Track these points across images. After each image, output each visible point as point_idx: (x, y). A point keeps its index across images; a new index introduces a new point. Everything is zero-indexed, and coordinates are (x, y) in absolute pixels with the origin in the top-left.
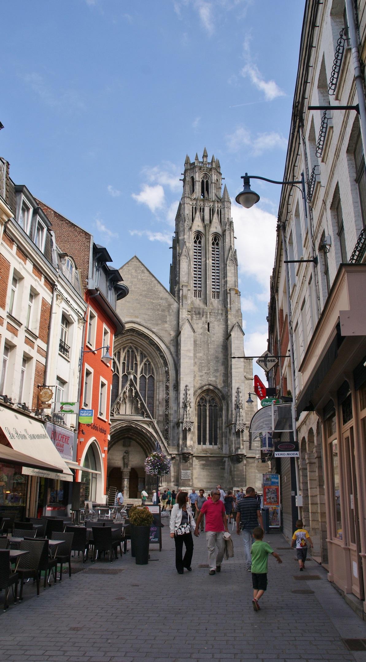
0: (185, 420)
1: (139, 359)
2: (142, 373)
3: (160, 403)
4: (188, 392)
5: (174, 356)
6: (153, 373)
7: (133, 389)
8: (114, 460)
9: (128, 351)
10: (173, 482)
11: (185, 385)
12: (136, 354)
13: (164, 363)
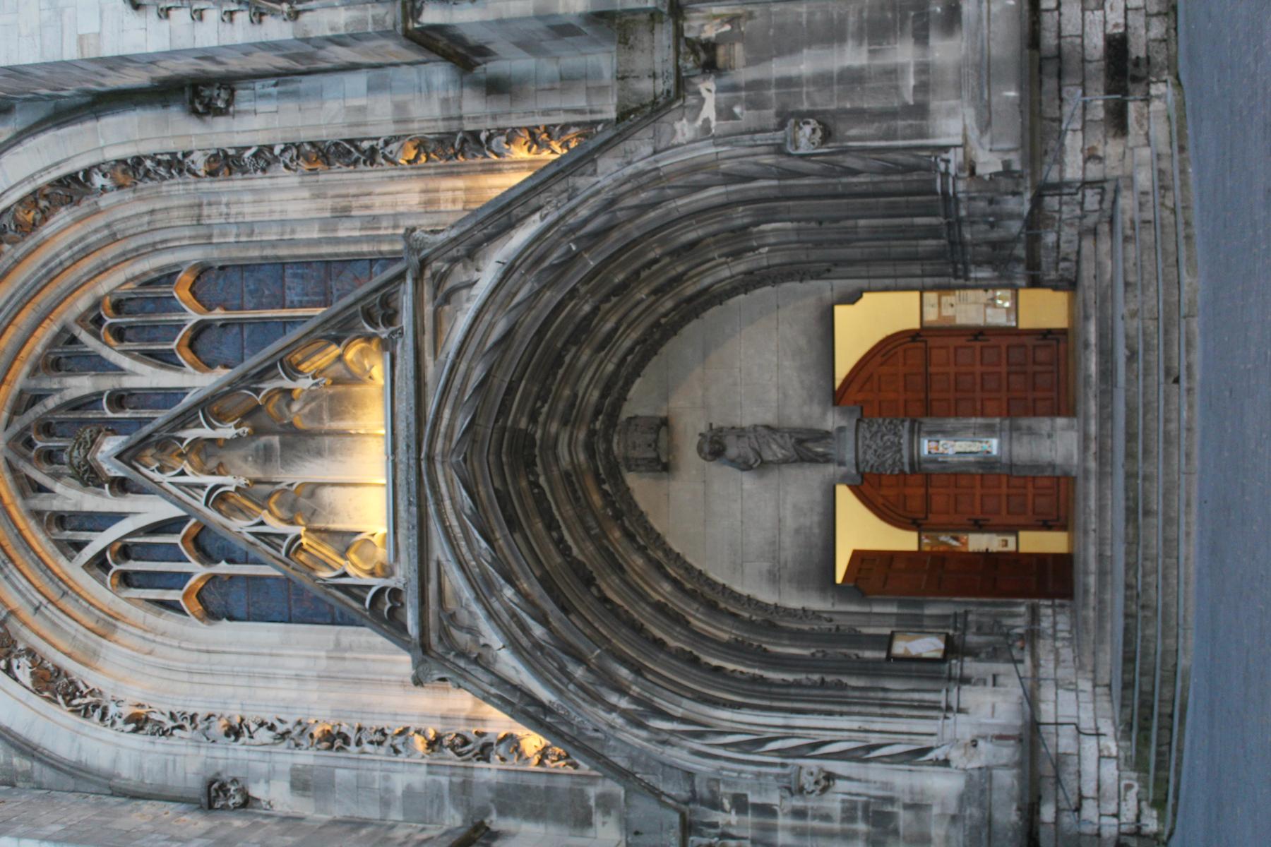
1: (81, 385)
2: (166, 360)
3: (343, 213)
6: (168, 276)
7: (190, 434)
9: (50, 456)
10: (921, 38)
12: (51, 402)
13: (71, 201)
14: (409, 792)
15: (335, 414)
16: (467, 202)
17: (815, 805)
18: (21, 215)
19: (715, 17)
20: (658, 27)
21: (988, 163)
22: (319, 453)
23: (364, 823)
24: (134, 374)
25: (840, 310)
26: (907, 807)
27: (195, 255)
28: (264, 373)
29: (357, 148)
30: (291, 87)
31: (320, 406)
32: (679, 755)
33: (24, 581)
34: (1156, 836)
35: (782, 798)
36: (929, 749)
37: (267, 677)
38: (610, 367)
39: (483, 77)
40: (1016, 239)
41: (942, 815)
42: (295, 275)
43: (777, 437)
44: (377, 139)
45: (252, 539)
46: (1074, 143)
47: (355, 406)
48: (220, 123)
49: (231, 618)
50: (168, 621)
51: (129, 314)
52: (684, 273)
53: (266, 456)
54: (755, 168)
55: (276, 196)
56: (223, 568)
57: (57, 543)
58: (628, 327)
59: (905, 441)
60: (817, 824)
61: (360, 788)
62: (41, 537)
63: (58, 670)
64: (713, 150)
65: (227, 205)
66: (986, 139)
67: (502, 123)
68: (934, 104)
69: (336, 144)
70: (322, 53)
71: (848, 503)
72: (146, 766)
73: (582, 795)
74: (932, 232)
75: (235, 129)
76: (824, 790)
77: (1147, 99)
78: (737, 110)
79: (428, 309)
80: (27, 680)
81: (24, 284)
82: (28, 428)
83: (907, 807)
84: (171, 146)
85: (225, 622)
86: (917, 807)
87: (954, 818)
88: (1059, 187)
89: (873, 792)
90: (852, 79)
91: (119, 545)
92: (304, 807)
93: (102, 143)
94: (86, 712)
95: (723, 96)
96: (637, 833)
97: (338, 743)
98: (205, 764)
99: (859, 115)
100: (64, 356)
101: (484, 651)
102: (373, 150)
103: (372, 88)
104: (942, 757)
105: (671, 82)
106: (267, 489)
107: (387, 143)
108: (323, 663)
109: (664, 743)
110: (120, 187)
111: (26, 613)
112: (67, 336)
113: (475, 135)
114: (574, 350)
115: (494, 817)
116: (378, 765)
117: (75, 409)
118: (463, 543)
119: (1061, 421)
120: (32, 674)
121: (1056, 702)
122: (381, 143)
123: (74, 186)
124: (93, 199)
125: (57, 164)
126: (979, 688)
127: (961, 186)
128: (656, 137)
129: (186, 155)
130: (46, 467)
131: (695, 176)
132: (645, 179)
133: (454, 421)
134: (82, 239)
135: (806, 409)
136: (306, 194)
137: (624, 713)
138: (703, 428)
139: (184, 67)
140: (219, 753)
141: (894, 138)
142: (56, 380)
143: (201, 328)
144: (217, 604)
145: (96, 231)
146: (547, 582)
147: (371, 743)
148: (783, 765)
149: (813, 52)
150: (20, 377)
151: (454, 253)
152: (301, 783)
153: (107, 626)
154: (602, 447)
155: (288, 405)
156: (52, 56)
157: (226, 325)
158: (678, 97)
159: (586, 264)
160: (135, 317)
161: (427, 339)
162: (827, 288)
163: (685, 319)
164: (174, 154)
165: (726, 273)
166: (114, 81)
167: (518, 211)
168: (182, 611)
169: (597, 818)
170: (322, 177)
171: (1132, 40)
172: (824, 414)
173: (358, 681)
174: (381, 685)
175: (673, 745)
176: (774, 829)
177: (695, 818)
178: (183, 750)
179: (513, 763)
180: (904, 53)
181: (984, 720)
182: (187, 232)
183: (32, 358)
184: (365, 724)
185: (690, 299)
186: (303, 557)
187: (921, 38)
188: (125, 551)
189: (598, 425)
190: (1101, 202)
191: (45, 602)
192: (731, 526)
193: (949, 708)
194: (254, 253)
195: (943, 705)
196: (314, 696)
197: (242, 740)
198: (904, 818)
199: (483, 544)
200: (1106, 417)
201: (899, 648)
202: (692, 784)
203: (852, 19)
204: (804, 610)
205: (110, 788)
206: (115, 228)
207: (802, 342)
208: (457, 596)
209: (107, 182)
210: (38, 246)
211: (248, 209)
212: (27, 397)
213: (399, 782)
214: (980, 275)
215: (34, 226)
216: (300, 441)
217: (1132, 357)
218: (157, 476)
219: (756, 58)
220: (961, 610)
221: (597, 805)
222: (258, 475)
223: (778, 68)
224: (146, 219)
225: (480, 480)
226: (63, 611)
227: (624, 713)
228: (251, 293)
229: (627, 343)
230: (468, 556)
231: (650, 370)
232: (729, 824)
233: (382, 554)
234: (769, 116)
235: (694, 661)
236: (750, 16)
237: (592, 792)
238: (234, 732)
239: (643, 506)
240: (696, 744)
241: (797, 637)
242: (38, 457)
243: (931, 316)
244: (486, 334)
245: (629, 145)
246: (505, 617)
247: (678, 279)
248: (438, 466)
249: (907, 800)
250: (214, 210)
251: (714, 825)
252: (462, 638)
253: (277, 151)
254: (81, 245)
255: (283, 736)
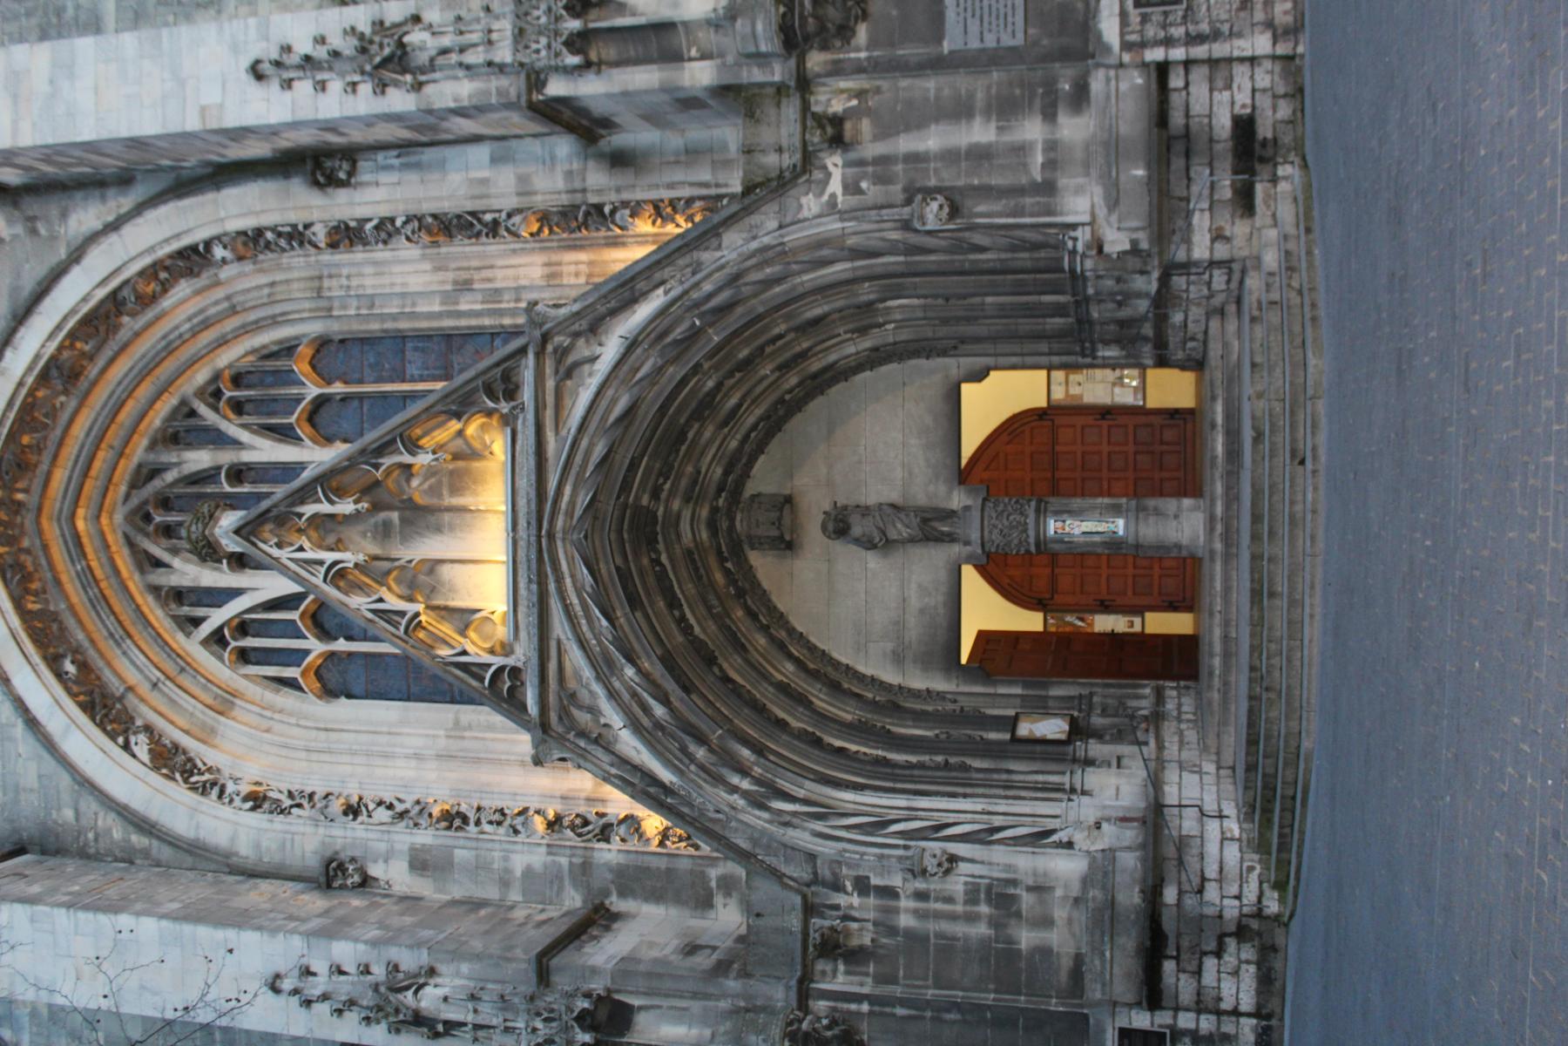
0: (504, 53)
1: (199, 459)
2: (284, 434)
3: (464, 286)
4: (304, 47)
5: (126, 202)
6: (288, 349)
7: (309, 510)
8: (899, 625)
9: (168, 531)
10: (1050, 116)
11: (253, 88)
12: (170, 476)
13: (191, 273)
14: (528, 872)
15: (455, 490)
16: (590, 276)
17: (939, 887)
18: (141, 287)
19: (842, 91)
20: (784, 101)
21: (1117, 241)
22: (439, 529)
23: (481, 904)
24: (252, 448)
25: (966, 388)
26: (1029, 889)
27: (315, 328)
28: (383, 448)
29: (479, 220)
30: (413, 159)
31: (440, 483)
32: (801, 837)
33: (142, 657)
34: (1277, 918)
35: (905, 880)
36: (1053, 832)
37: (386, 756)
38: (734, 444)
39: (607, 149)
40: (1144, 318)
41: (1065, 898)
42: (416, 349)
43: (902, 516)
44: (500, 211)
45: (370, 616)
46: (1201, 223)
47: (475, 482)
48: (342, 195)
49: (350, 696)
50: (286, 699)
51: (249, 387)
52: (810, 349)
53: (385, 532)
54: (880, 244)
55: (397, 269)
56: (341, 645)
57: (175, 618)
58: (753, 402)
59: (1031, 520)
60: (939, 906)
61: (480, 868)
62: (159, 612)
63: (176, 747)
64: (839, 225)
65: (348, 277)
66: (1114, 218)
67: (626, 196)
68: (1063, 182)
69: (459, 217)
70: (445, 125)
71: (973, 583)
72: (265, 844)
73: (703, 876)
74: (1059, 310)
75: (357, 200)
76: (947, 872)
77: (1274, 180)
78: (864, 185)
79: (550, 384)
80: (145, 757)
81: (143, 356)
82: (146, 502)
83: (1029, 889)
84: (294, 217)
85: (343, 700)
86: (1040, 889)
87: (1077, 900)
88: (1186, 267)
89: (996, 875)
90: (980, 155)
91: (237, 621)
92: (422, 887)
93: (223, 214)
94: (204, 789)
95: (850, 171)
96: (758, 915)
97: (457, 822)
98: (323, 843)
99: (986, 192)
100: (183, 430)
101: (604, 731)
102: (496, 222)
103: (495, 160)
104: (1065, 840)
105: (798, 156)
106: (386, 565)
107: (509, 216)
108: (442, 742)
109: (787, 824)
110: (240, 258)
111: (144, 689)
112: (185, 410)
113: (599, 208)
114: (696, 426)
115: (614, 898)
116: (497, 846)
117: (194, 483)
118: (583, 622)
119: (1187, 502)
120: (150, 751)
121: (1180, 784)
122: (504, 215)
123: (195, 258)
124: (212, 271)
125: (177, 236)
126: (1103, 770)
127: (1089, 264)
128: (781, 211)
129: (307, 226)
130: (164, 542)
131: (820, 251)
132: (770, 254)
133: (575, 498)
134: (202, 311)
135: (931, 488)
136: (427, 266)
137: (746, 794)
138: (827, 507)
139: (305, 138)
140: (337, 831)
141: (1022, 215)
142: (174, 454)
143: (321, 402)
144: (335, 681)
145: (216, 303)
146: (668, 661)
147: (490, 822)
148: (906, 847)
149: (940, 128)
150: (139, 451)
151: (576, 327)
152: (420, 863)
153: (225, 702)
154: (725, 525)
155: (408, 481)
156: (174, 127)
157: (346, 398)
158: (804, 171)
159: (711, 339)
160: (254, 391)
161: (549, 414)
162: (953, 365)
163: (809, 396)
164: (294, 226)
165: (851, 349)
166: (236, 152)
167: (641, 285)
168: (300, 689)
169: (719, 900)
170: (443, 250)
171: (1259, 121)
172: (950, 492)
173: (477, 761)
174: (499, 764)
175: (795, 827)
176: (896, 911)
177: (817, 900)
178: (302, 829)
179: (634, 844)
180: (1032, 130)
181: (1108, 803)
182: (307, 305)
183: (151, 432)
184: (484, 803)
185: (815, 376)
186: (422, 634)
187: (1050, 116)
188: (243, 627)
189: (721, 501)
190: (1228, 282)
191: (162, 678)
192: (856, 606)
193: (1073, 790)
194: (375, 326)
195: (1067, 787)
196: (433, 776)
197: (360, 819)
198: (1027, 900)
199: (604, 623)
200: (1232, 497)
201: (1024, 729)
202: (815, 866)
203: (980, 95)
204: (928, 690)
205: (228, 866)
206: (235, 300)
207: (929, 420)
208: (578, 678)
209: (228, 254)
210: (158, 318)
211: (368, 282)
212: (145, 471)
213: (519, 862)
214: (1108, 353)
215: (154, 298)
216: (420, 516)
217: (1258, 438)
218: (275, 552)
219: (886, 131)
220: (1085, 692)
221: (718, 887)
222: (375, 550)
223: (906, 143)
224: (266, 291)
225: (600, 556)
226: (180, 687)
227: (746, 794)
228: (370, 366)
229: (751, 420)
230: (589, 635)
231: (774, 447)
232: (851, 907)
233: (502, 632)
234: (896, 191)
235: (817, 742)
236: (878, 90)
237: (714, 873)
238: (352, 811)
239: (765, 584)
240: (819, 826)
241: (919, 717)
242: (156, 530)
243: (1059, 394)
244: (609, 410)
245: (755, 219)
246: (626, 696)
247: (803, 355)
248: (559, 544)
249: (1030, 882)
250: (334, 283)
251: (837, 907)
252: (583, 718)
253: (399, 223)
254: (200, 318)
255: (402, 815)
